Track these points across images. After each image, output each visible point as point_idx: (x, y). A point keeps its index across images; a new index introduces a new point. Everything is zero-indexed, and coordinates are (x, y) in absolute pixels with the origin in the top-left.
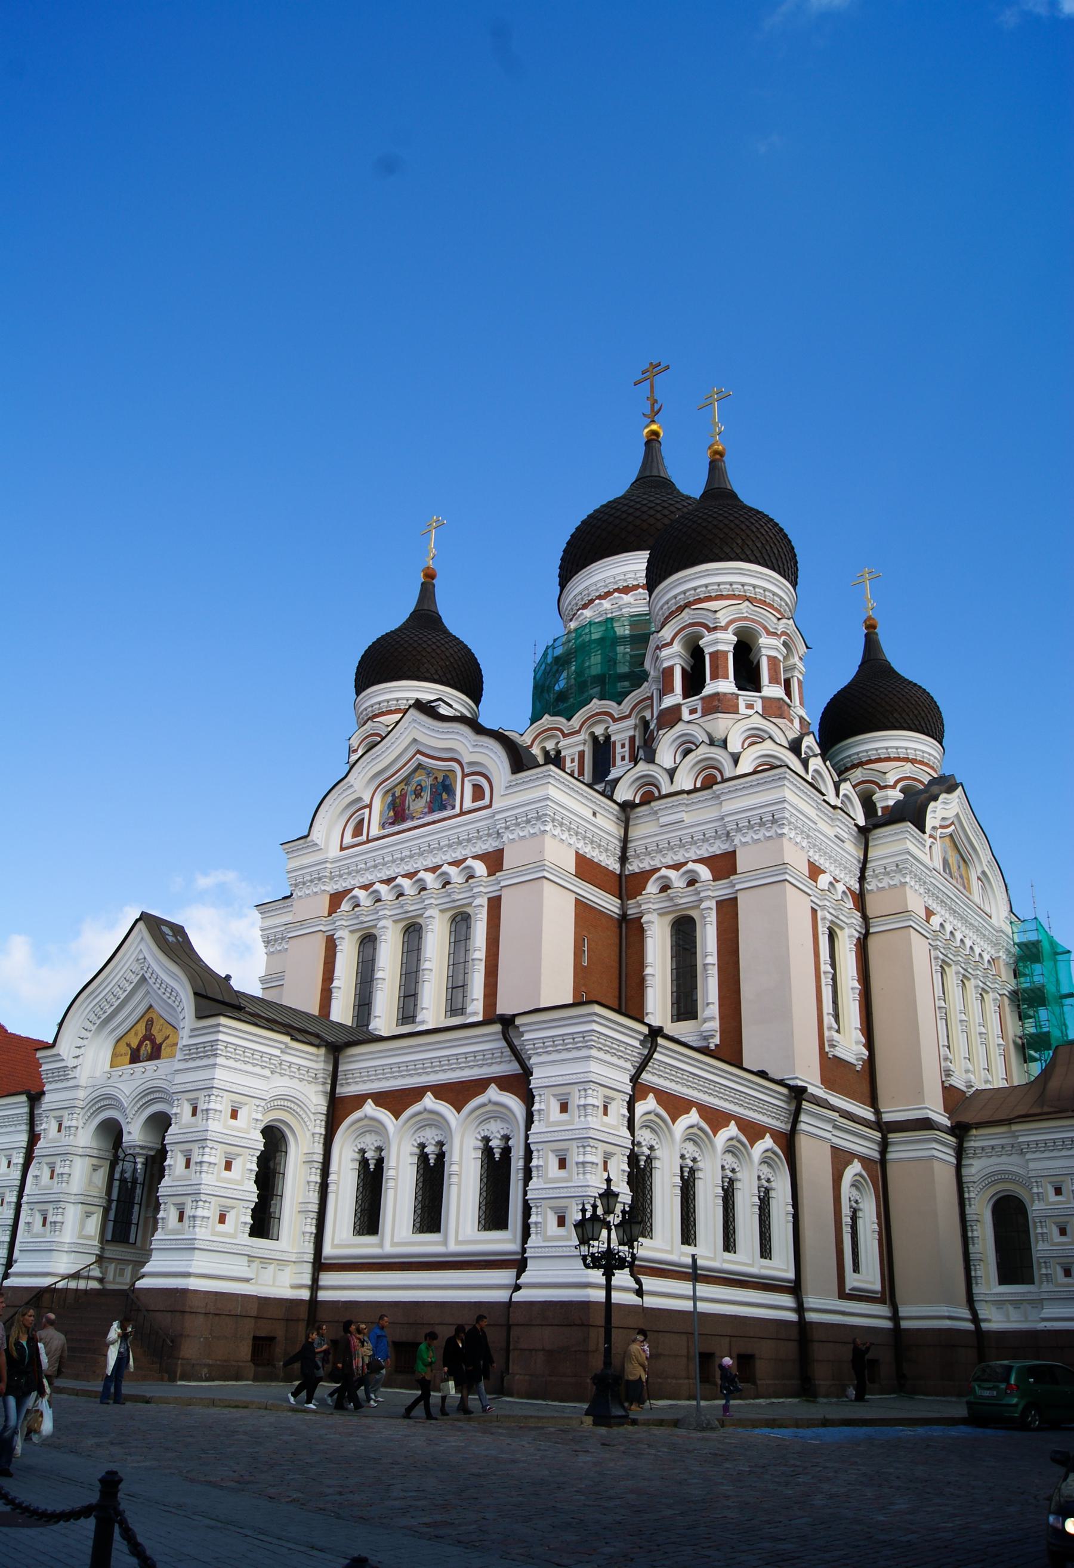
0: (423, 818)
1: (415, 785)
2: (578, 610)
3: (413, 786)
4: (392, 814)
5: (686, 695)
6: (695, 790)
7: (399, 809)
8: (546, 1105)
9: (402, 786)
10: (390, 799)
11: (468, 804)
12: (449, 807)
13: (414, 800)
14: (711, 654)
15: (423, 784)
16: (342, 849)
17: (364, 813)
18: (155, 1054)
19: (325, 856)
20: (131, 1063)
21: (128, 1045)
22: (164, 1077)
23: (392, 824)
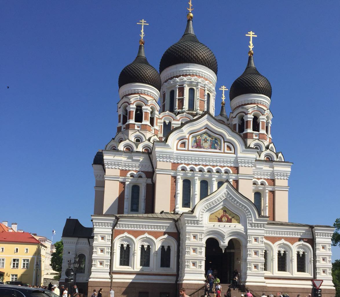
0: (208, 149)
1: (204, 138)
2: (180, 76)
3: (203, 138)
4: (195, 144)
5: (253, 130)
6: (266, 161)
7: (199, 144)
8: (319, 247)
9: (199, 137)
10: (194, 139)
11: (226, 151)
12: (218, 149)
13: (204, 143)
14: (262, 121)
15: (208, 139)
16: (177, 150)
17: (186, 141)
18: (229, 221)
19: (173, 151)
20: (218, 222)
21: (216, 216)
22: (240, 229)
23: (196, 147)
